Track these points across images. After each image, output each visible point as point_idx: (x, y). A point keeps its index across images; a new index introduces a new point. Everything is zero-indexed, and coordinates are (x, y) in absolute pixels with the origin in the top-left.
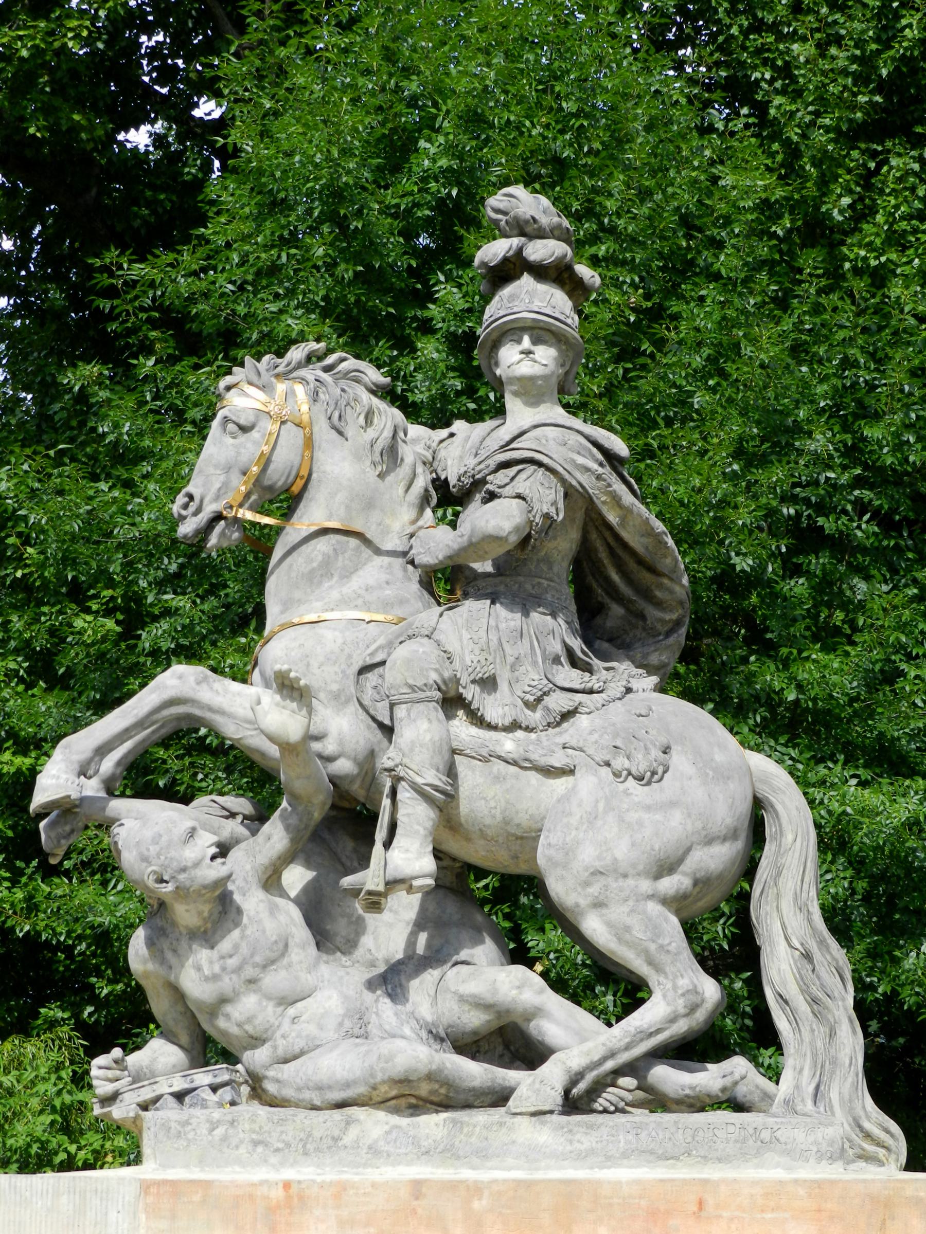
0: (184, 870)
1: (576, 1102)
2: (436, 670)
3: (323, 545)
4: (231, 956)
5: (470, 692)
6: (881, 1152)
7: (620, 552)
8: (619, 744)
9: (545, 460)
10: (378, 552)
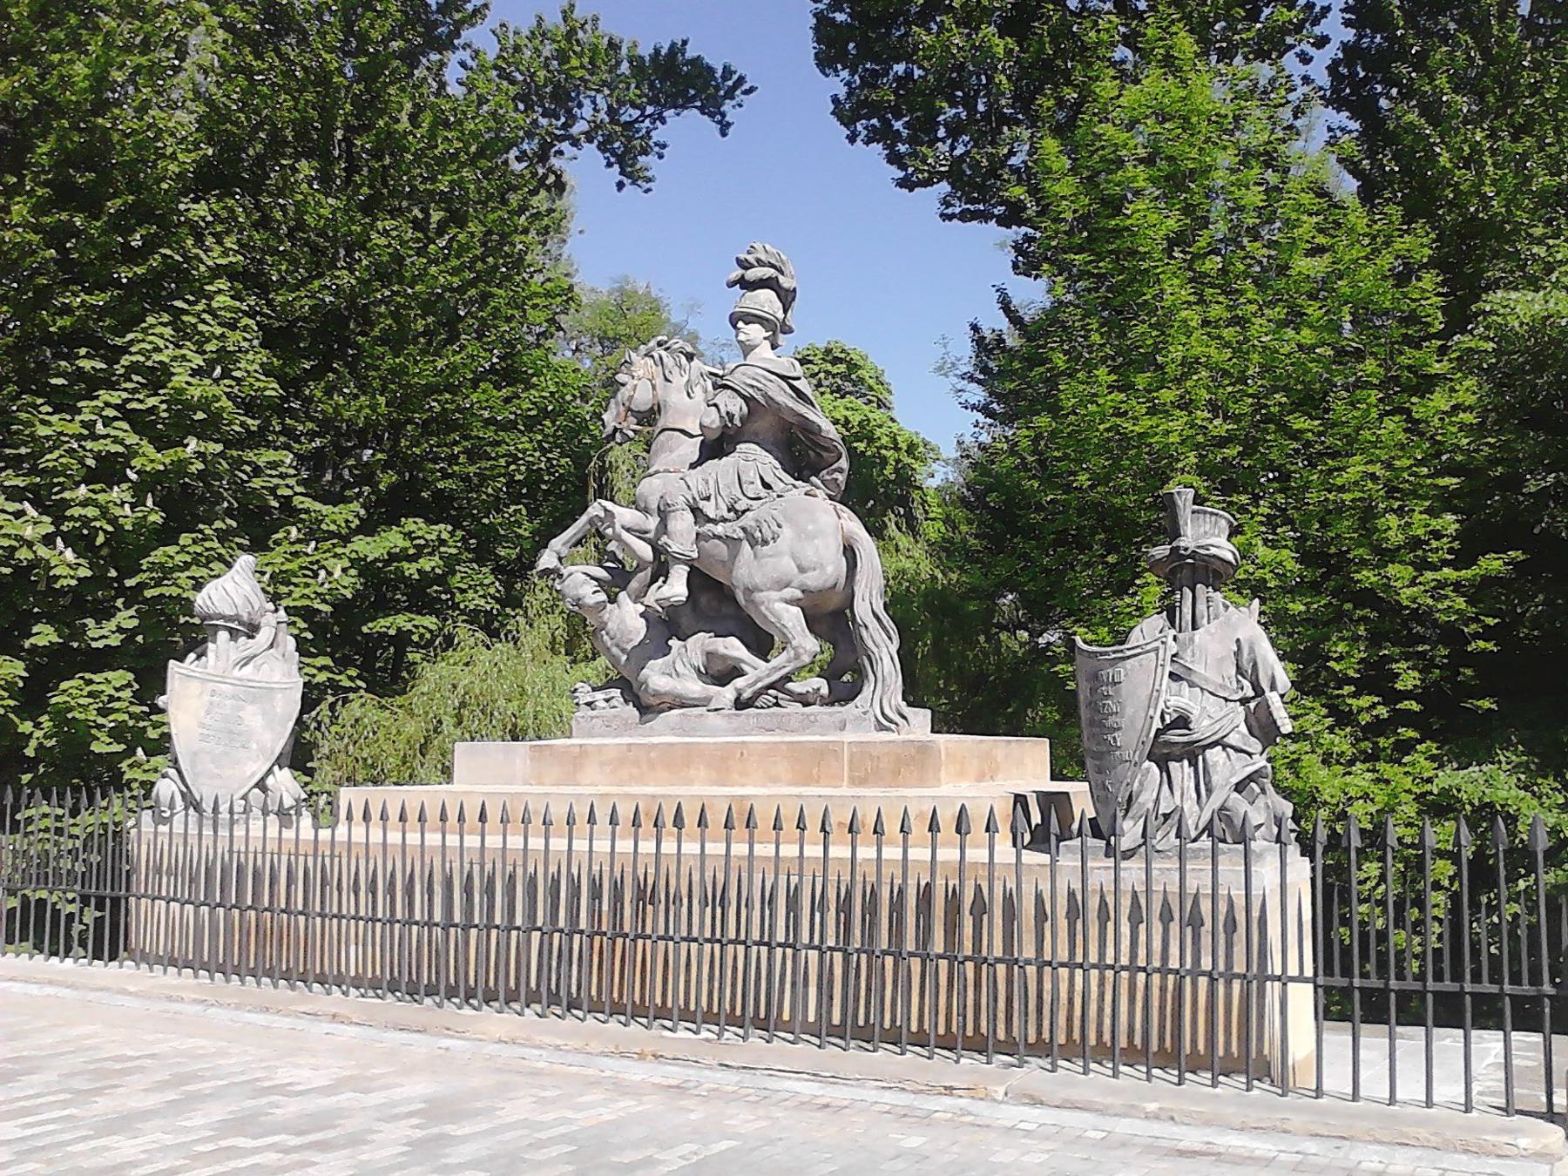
1: (740, 704)
3: (662, 437)
5: (702, 504)
10: (692, 436)
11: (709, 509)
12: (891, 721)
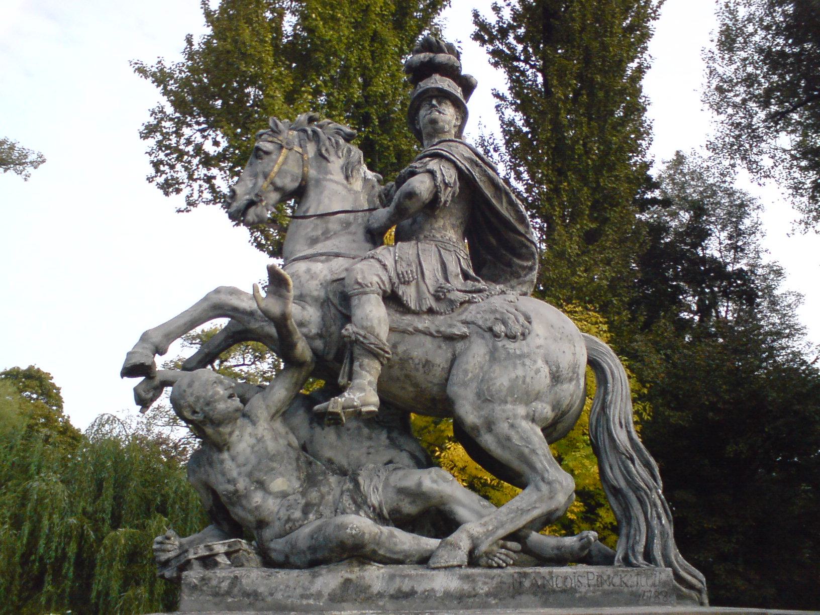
0: (208, 404)
2: (378, 276)
4: (244, 465)
6: (694, 594)
7: (493, 220)
8: (498, 316)
9: (444, 153)
11: (409, 294)
12: (691, 587)
